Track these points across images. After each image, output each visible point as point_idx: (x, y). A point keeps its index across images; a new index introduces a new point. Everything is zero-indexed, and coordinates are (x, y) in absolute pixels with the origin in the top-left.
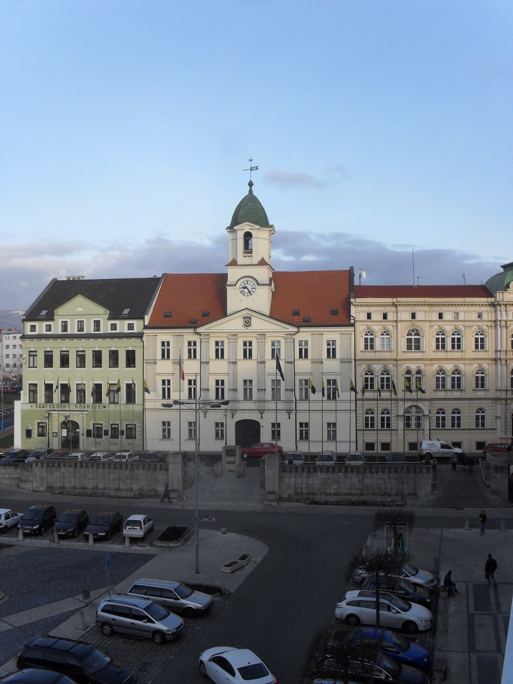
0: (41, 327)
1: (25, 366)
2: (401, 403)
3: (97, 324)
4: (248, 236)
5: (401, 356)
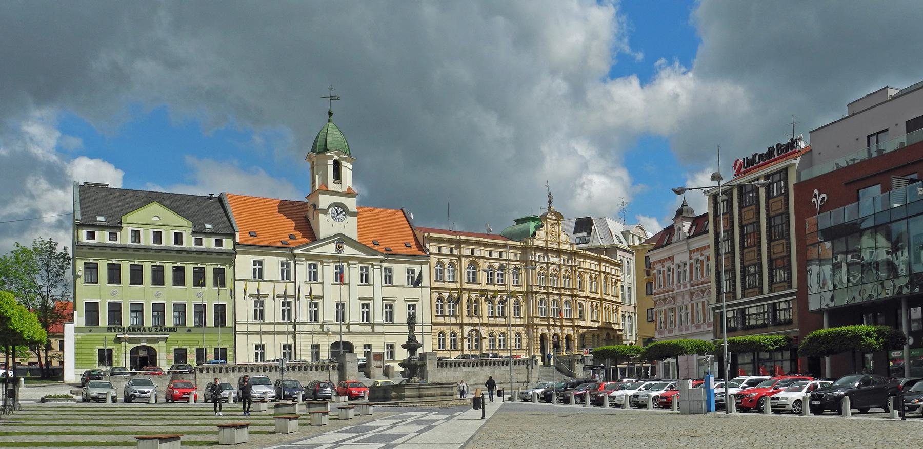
0: (102, 237)
1: (80, 282)
2: (465, 327)
3: (178, 238)
4: (337, 165)
5: (465, 286)
